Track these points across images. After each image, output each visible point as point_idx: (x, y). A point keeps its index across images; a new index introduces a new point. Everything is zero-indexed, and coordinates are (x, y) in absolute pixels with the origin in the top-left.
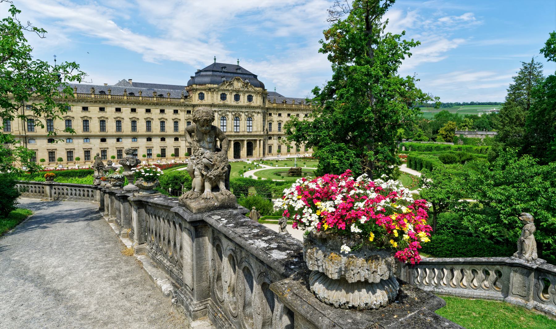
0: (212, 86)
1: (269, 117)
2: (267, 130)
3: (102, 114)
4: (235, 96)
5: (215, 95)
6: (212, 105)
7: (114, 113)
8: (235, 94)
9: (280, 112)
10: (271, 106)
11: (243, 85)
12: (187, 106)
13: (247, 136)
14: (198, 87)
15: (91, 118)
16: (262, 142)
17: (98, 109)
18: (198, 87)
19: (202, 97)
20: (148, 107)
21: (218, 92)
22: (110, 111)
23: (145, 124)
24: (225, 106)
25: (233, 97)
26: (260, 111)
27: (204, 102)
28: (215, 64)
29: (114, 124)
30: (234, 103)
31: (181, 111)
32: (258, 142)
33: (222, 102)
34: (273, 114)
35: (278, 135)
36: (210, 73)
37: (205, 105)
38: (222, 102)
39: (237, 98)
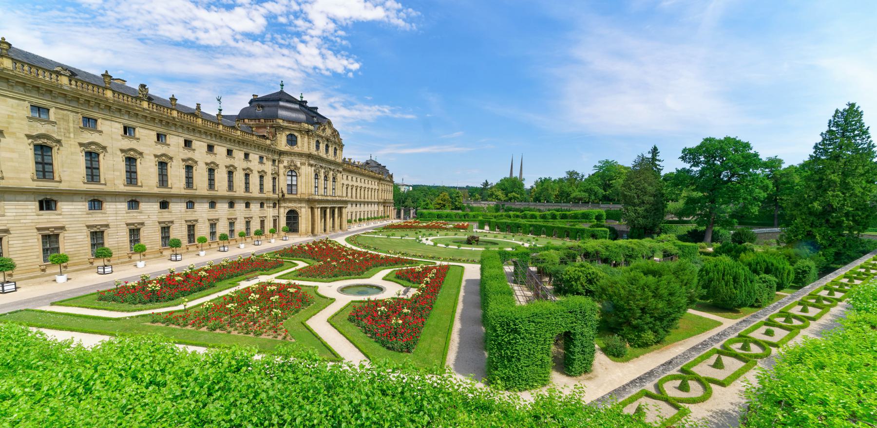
3: (161, 149)
5: (311, 141)
6: (310, 156)
7: (181, 149)
12: (274, 152)
14: (286, 124)
15: (141, 154)
18: (286, 124)
19: (292, 140)
20: (230, 147)
22: (175, 141)
24: (321, 159)
27: (296, 149)
28: (282, 92)
29: (183, 172)
36: (297, 106)
37: (300, 155)
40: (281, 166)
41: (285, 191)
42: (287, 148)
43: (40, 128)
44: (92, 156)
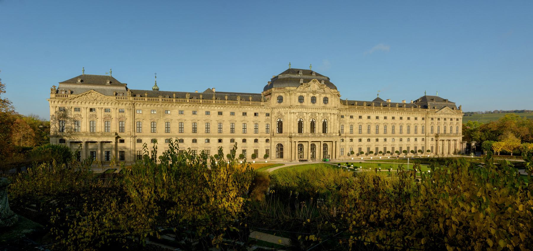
1: (341, 119)
2: (339, 132)
8: (311, 95)
17: (191, 112)
19: (280, 99)
20: (232, 110)
29: (204, 126)
31: (261, 113)
34: (345, 117)
38: (299, 104)
39: (314, 100)
40: (273, 116)
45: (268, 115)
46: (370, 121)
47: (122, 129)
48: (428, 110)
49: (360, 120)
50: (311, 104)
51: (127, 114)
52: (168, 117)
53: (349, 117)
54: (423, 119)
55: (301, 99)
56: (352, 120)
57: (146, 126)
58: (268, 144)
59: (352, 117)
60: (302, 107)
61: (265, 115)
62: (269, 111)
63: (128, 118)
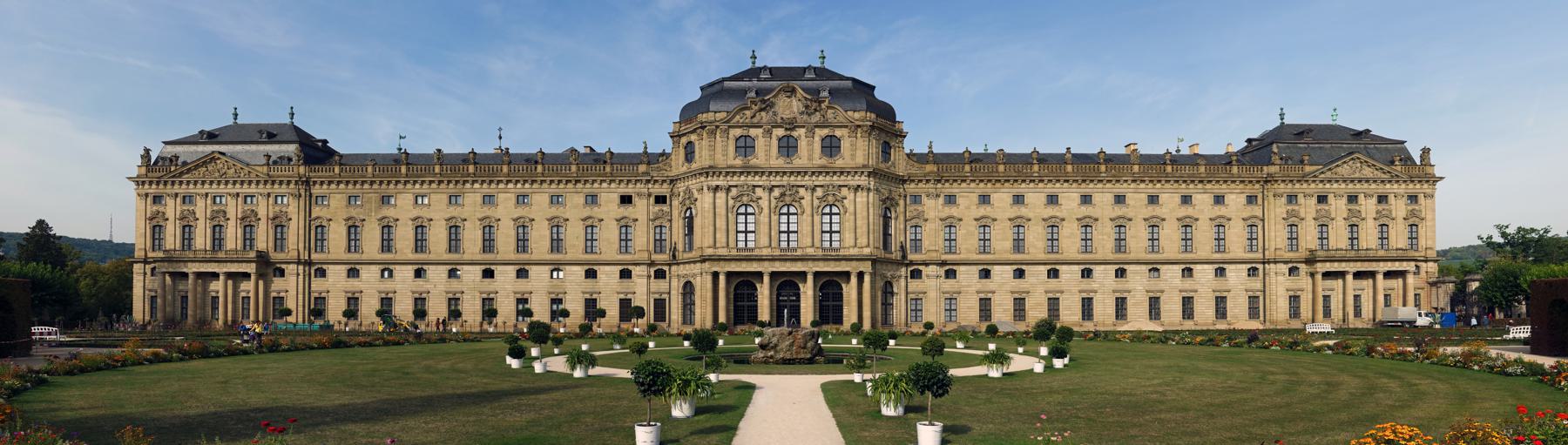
0: (710, 116)
2: (903, 248)
3: (454, 211)
4: (779, 140)
8: (780, 132)
9: (948, 189)
10: (915, 170)
11: (807, 107)
13: (814, 259)
16: (867, 278)
21: (726, 132)
22: (472, 198)
23: (548, 233)
25: (775, 142)
26: (862, 180)
30: (778, 162)
31: (639, 195)
32: (854, 280)
33: (738, 162)
35: (943, 263)
39: (788, 147)
40: (675, 203)
41: (680, 247)
42: (684, 169)
43: (353, 212)
44: (387, 228)
45: (660, 200)
46: (1023, 211)
47: (280, 242)
48: (1273, 169)
49: (983, 211)
50: (778, 162)
51: (293, 208)
52: (388, 212)
53: (941, 200)
54: (1251, 200)
55: (745, 146)
56: (954, 211)
57: (337, 236)
58: (662, 285)
59: (951, 200)
60: (747, 171)
61: (652, 200)
62: (664, 190)
63: (294, 218)
